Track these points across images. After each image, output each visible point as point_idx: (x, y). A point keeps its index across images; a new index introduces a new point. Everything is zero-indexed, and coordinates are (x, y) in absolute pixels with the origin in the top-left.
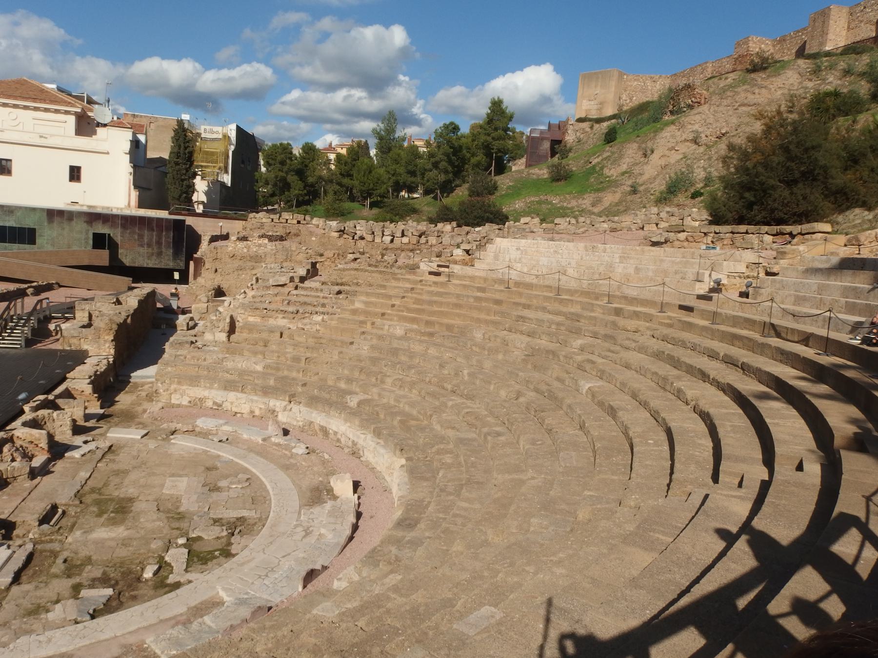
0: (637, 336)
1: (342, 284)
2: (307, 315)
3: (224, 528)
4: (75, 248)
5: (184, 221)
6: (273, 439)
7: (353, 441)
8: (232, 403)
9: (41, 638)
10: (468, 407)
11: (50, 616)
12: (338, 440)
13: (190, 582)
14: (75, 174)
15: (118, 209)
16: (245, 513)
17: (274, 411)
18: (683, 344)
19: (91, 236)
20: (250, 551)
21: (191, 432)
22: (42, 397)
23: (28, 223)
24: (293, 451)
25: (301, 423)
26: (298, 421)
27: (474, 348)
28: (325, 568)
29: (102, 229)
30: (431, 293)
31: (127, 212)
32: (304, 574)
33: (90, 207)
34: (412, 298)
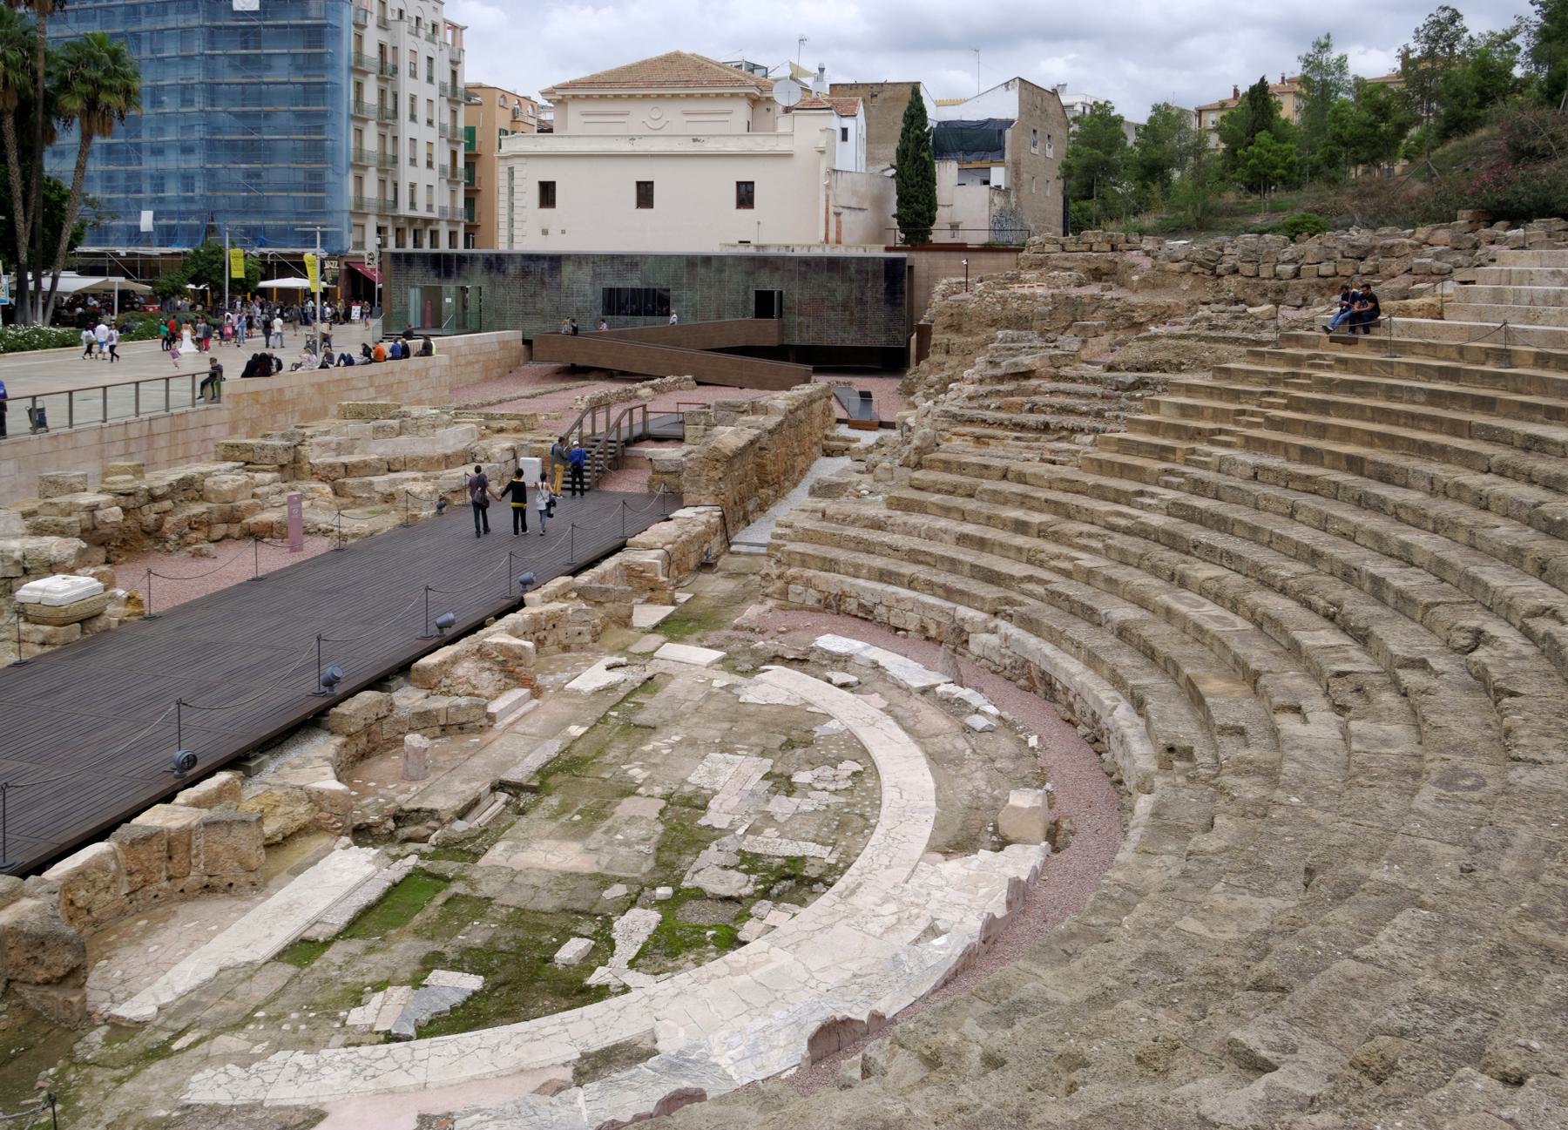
1: (1148, 368)
2: (1064, 433)
3: (753, 877)
5: (903, 260)
6: (939, 689)
7: (1094, 713)
8: (889, 608)
10: (1348, 660)
12: (1070, 706)
14: (745, 196)
15: (779, 246)
16: (811, 849)
17: (962, 630)
19: (752, 297)
21: (800, 662)
23: (658, 281)
25: (1007, 661)
26: (1003, 656)
27: (1402, 513)
29: (771, 283)
30: (1328, 385)
31: (818, 252)
33: (758, 247)
34: (1283, 396)
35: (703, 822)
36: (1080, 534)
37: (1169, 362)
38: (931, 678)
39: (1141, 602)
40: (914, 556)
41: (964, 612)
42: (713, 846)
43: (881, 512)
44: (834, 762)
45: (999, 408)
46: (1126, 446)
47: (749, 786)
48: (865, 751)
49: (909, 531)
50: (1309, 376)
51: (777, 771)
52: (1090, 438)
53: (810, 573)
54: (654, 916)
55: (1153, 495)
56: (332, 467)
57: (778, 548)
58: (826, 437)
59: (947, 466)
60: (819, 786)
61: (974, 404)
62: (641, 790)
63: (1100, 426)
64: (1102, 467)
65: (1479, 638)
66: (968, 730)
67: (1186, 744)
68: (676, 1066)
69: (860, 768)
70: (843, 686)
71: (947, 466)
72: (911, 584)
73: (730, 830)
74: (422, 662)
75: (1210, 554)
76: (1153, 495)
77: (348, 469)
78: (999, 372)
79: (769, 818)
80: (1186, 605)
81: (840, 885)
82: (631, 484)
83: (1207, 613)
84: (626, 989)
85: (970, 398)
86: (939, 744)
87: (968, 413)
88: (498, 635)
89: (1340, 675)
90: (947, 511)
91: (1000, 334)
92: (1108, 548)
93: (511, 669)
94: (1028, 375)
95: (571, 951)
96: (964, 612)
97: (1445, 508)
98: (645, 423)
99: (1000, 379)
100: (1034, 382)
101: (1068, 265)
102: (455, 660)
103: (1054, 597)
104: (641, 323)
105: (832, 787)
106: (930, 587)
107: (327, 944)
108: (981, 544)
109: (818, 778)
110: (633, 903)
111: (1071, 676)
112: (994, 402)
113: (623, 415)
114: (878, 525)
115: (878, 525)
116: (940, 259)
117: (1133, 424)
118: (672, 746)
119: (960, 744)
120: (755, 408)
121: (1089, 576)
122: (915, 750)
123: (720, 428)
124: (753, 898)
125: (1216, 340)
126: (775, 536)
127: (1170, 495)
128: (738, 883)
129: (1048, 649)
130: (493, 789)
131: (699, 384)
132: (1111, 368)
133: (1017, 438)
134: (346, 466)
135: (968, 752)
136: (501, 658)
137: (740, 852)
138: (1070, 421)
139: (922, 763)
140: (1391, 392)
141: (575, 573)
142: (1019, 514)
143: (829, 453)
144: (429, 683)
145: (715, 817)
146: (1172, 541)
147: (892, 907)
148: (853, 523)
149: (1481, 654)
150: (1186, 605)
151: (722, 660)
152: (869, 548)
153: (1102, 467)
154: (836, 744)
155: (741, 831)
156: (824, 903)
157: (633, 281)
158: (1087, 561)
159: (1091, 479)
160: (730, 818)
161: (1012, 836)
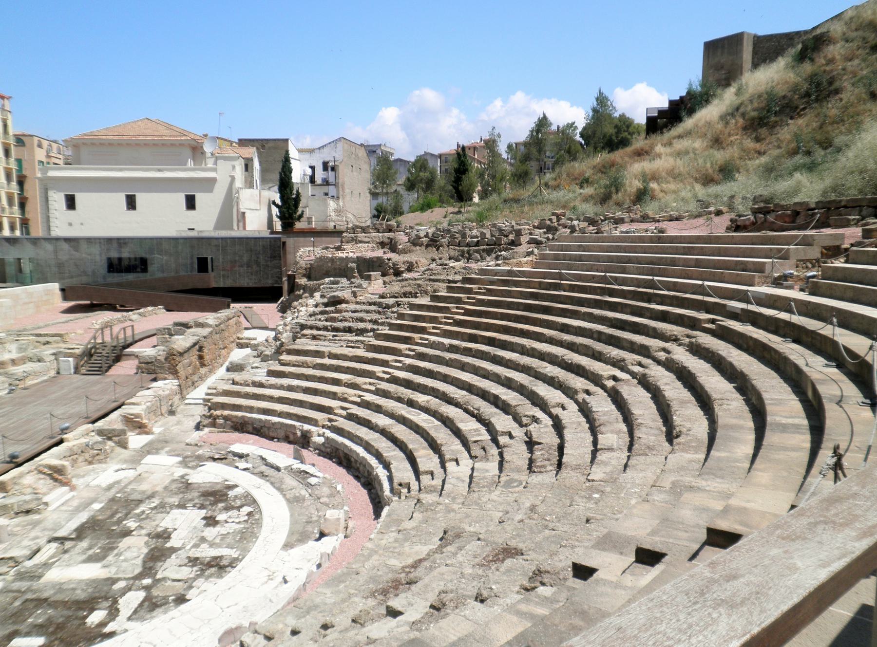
4: (182, 273)
19: (196, 261)
26: (326, 448)
34: (462, 308)
35: (168, 545)
36: (365, 383)
37: (410, 293)
41: (306, 427)
42: (173, 556)
44: (239, 508)
45: (326, 320)
46: (388, 338)
47: (193, 525)
48: (254, 501)
50: (474, 298)
51: (208, 515)
52: (371, 334)
53: (226, 413)
54: (142, 595)
55: (400, 362)
57: (209, 400)
58: (238, 338)
60: (231, 521)
61: (313, 318)
62: (134, 533)
63: (375, 327)
66: (310, 485)
67: (407, 481)
69: (252, 510)
70: (245, 469)
72: (281, 414)
76: (400, 362)
78: (326, 300)
79: (203, 540)
82: (126, 368)
84: (126, 631)
85: (311, 315)
87: (309, 323)
88: (49, 458)
89: (475, 442)
91: (327, 280)
92: (377, 389)
94: (340, 301)
95: (96, 617)
96: (306, 427)
99: (326, 305)
100: (344, 306)
101: (367, 240)
102: (21, 476)
103: (351, 417)
104: (131, 277)
105: (237, 521)
109: (230, 517)
110: (130, 589)
112: (323, 317)
113: (121, 330)
114: (261, 385)
115: (261, 385)
117: (392, 326)
118: (152, 509)
119: (303, 492)
122: (280, 497)
123: (176, 337)
124: (195, 579)
125: (434, 280)
126: (208, 394)
127: (408, 361)
130: (49, 541)
131: (168, 310)
132: (382, 297)
133: (334, 336)
135: (307, 496)
136: (50, 472)
137: (189, 557)
138: (361, 325)
139: (284, 503)
140: (510, 306)
141: (94, 422)
143: (241, 346)
145: (173, 543)
146: (408, 384)
147: (266, 573)
148: (248, 385)
151: (180, 463)
154: (240, 499)
155: (188, 547)
156: (232, 575)
158: (368, 397)
160: (182, 541)
161: (326, 531)
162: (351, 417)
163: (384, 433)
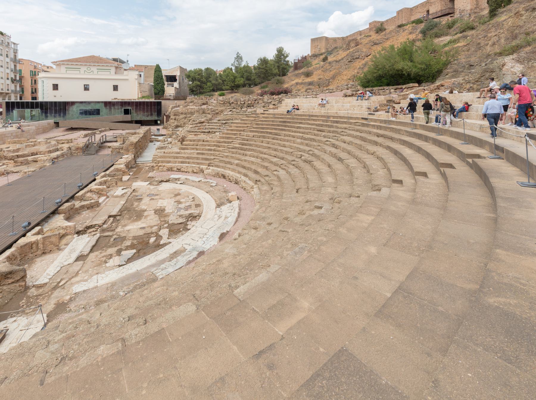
0: (346, 131)
9: (103, 275)
11: (107, 265)
12: (230, 179)
13: (170, 243)
18: (366, 132)
20: (195, 227)
22: (103, 174)
24: (212, 184)
28: (228, 232)
32: (219, 234)
38: (200, 179)
39: (239, 160)
40: (188, 158)
43: (179, 151)
49: (185, 153)
56: (13, 156)
59: (191, 141)
64: (223, 138)
65: (301, 156)
68: (194, 249)
71: (191, 141)
73: (173, 212)
74: (77, 195)
75: (250, 150)
77: (18, 156)
80: (247, 158)
81: (203, 215)
83: (253, 159)
86: (207, 189)
88: (93, 186)
90: (193, 149)
93: (99, 193)
96: (202, 166)
97: (286, 138)
98: (106, 138)
102: (85, 193)
103: (221, 161)
106: (194, 163)
107: (88, 255)
108: (203, 154)
110: (160, 229)
111: (229, 174)
116: (167, 102)
119: (211, 189)
120: (135, 133)
121: (227, 157)
122: (203, 191)
127: (239, 141)
128: (181, 220)
129: (223, 170)
134: (17, 156)
142: (209, 148)
144: (82, 199)
146: (242, 149)
149: (303, 158)
150: (247, 158)
152: (177, 158)
153: (223, 138)
157: (88, 108)
158: (226, 154)
159: (222, 140)
162: (221, 161)
163: (237, 165)
